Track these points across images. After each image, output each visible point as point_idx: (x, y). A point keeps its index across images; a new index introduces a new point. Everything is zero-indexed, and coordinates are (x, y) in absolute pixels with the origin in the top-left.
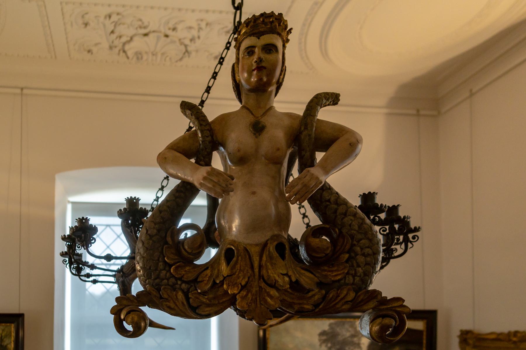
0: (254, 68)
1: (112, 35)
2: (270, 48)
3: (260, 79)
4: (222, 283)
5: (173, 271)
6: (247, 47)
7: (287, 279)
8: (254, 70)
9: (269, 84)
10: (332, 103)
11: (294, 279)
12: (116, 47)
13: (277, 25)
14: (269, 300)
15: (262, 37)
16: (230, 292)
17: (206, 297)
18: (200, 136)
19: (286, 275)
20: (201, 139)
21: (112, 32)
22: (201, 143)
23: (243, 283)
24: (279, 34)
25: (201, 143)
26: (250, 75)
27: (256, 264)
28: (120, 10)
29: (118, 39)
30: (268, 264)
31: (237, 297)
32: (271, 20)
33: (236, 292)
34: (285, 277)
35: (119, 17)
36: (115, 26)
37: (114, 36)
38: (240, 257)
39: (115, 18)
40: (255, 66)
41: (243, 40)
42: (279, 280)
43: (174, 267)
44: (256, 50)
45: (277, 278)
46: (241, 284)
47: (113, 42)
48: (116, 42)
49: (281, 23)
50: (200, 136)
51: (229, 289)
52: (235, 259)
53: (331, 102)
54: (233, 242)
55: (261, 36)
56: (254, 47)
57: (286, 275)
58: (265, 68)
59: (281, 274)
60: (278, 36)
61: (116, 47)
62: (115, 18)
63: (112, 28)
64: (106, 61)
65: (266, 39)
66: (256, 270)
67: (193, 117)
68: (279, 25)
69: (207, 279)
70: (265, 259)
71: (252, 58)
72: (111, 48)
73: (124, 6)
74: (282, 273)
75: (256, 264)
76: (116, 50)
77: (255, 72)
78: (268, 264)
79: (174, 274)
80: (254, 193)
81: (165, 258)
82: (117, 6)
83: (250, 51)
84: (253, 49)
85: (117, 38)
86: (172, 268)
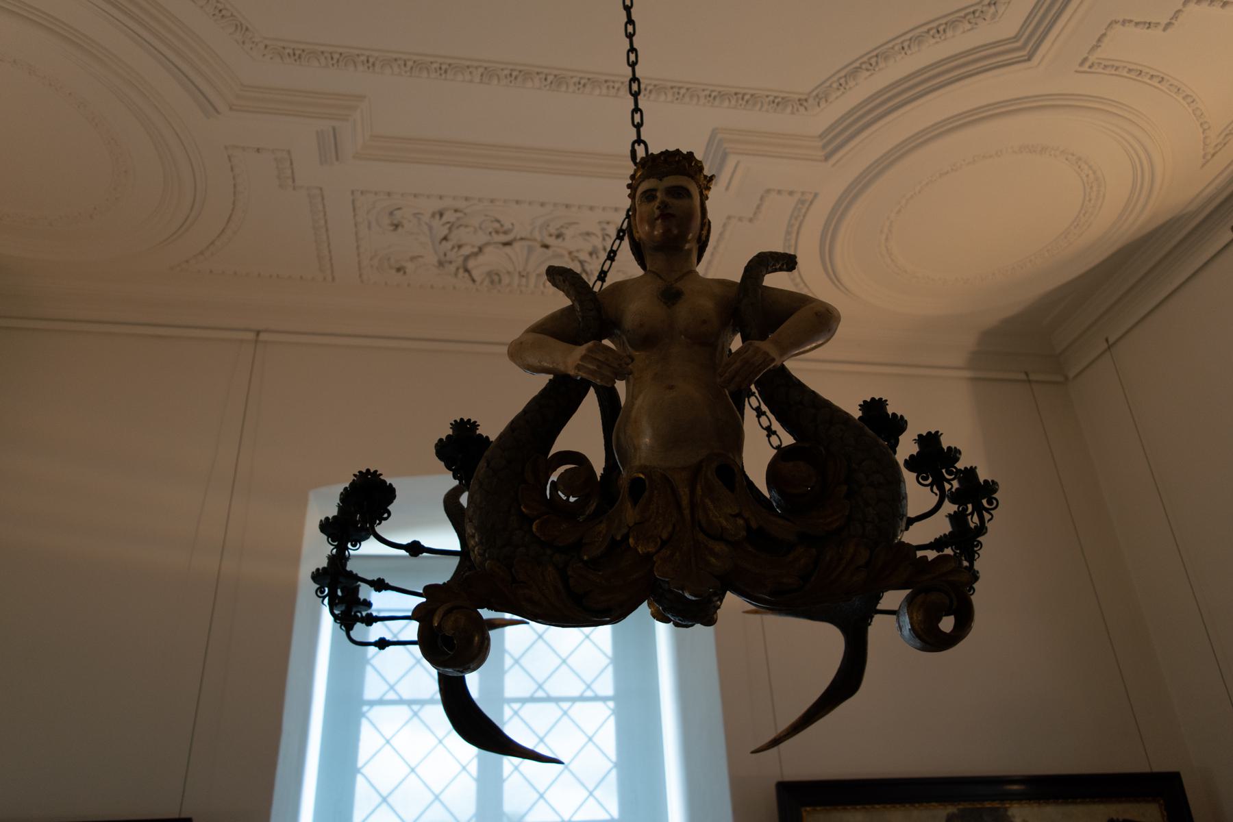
0: (656, 216)
1: (444, 242)
2: (680, 192)
3: (667, 231)
4: (626, 538)
5: (537, 529)
6: (643, 190)
7: (740, 522)
8: (657, 219)
9: (682, 237)
10: (785, 266)
11: (754, 525)
12: (451, 262)
13: (687, 165)
14: (713, 560)
15: (665, 179)
16: (642, 550)
17: (600, 573)
18: (578, 310)
19: (739, 515)
20: (580, 314)
21: (445, 238)
22: (580, 320)
23: (665, 536)
24: (693, 178)
25: (580, 320)
26: (652, 225)
27: (685, 501)
28: (461, 204)
29: (456, 250)
30: (707, 500)
31: (655, 559)
32: (677, 159)
33: (651, 549)
34: (738, 519)
35: (458, 215)
36: (450, 229)
37: (447, 245)
38: (656, 492)
39: (449, 216)
40: (657, 212)
41: (639, 184)
42: (728, 527)
43: (537, 521)
44: (659, 194)
45: (724, 523)
46: (660, 537)
47: (445, 255)
48: (452, 255)
49: (692, 163)
50: (578, 310)
51: (638, 546)
52: (647, 494)
53: (783, 265)
54: (643, 469)
55: (663, 177)
56: (655, 190)
57: (739, 515)
58: (673, 216)
59: (731, 515)
60: (690, 179)
61: (451, 262)
62: (449, 216)
63: (445, 231)
64: (432, 287)
65: (671, 181)
66: (687, 512)
67: (567, 282)
68: (690, 165)
69: (601, 539)
70: (700, 493)
71: (652, 204)
72: (441, 264)
73: (467, 199)
74: (733, 513)
75: (685, 501)
76: (452, 268)
77: (660, 221)
78: (707, 500)
79: (538, 534)
80: (671, 387)
81: (522, 507)
82: (454, 198)
83: (649, 195)
84: (654, 193)
85: (453, 248)
86: (535, 523)
